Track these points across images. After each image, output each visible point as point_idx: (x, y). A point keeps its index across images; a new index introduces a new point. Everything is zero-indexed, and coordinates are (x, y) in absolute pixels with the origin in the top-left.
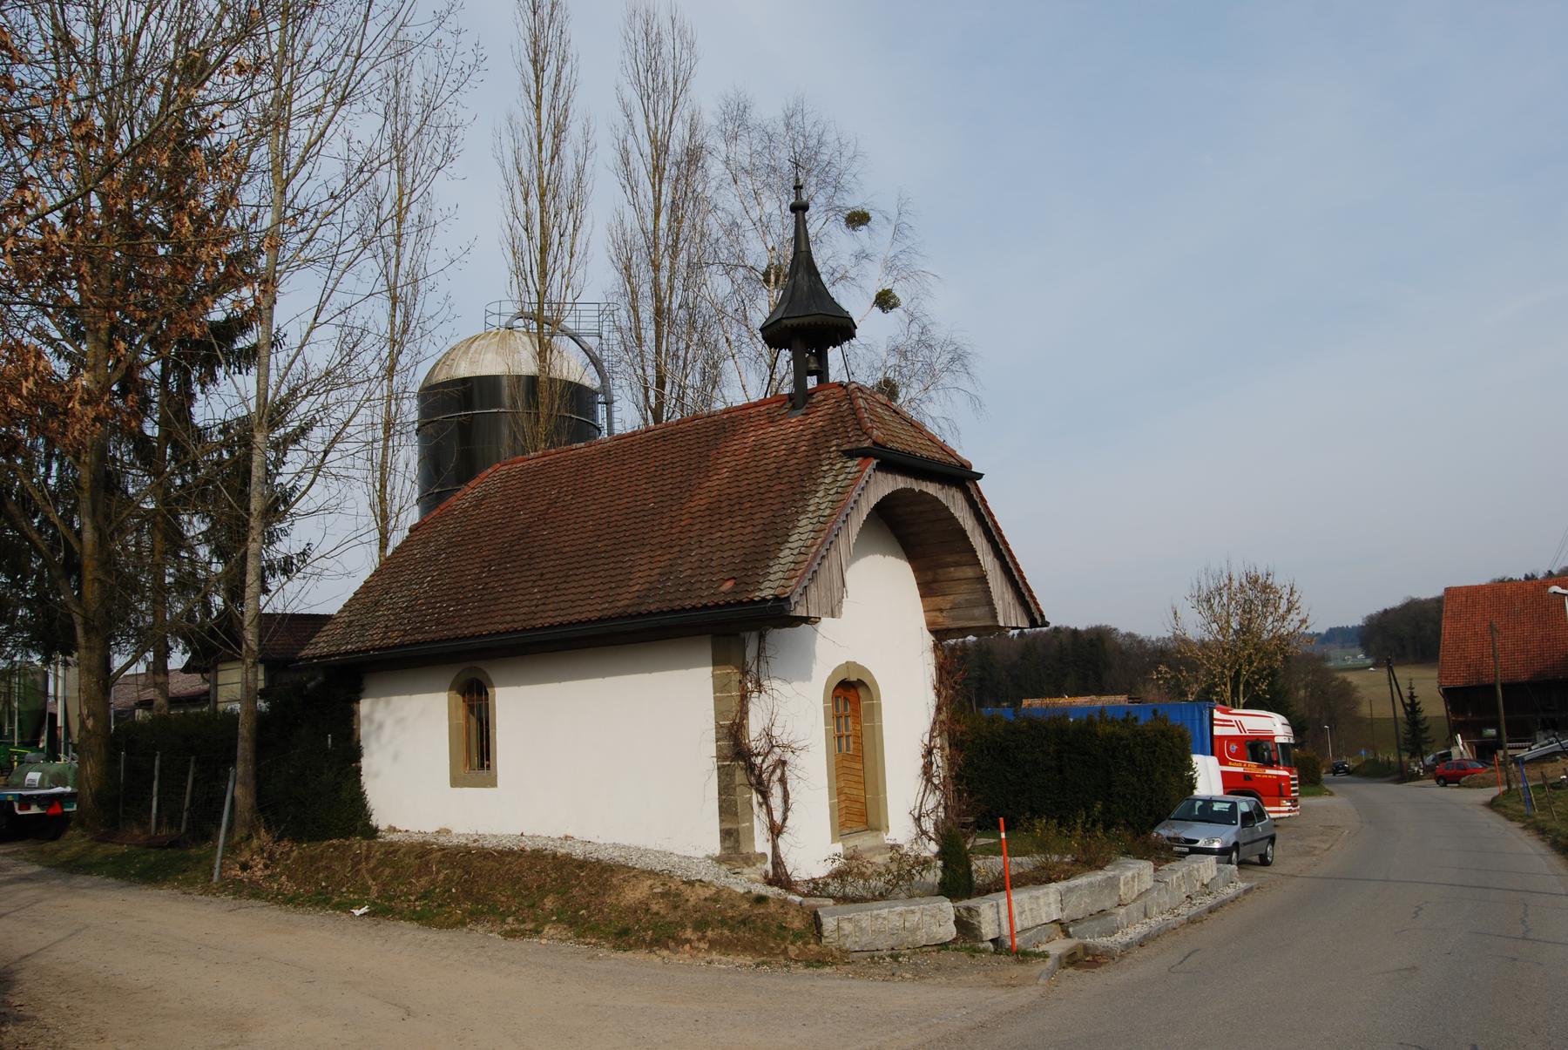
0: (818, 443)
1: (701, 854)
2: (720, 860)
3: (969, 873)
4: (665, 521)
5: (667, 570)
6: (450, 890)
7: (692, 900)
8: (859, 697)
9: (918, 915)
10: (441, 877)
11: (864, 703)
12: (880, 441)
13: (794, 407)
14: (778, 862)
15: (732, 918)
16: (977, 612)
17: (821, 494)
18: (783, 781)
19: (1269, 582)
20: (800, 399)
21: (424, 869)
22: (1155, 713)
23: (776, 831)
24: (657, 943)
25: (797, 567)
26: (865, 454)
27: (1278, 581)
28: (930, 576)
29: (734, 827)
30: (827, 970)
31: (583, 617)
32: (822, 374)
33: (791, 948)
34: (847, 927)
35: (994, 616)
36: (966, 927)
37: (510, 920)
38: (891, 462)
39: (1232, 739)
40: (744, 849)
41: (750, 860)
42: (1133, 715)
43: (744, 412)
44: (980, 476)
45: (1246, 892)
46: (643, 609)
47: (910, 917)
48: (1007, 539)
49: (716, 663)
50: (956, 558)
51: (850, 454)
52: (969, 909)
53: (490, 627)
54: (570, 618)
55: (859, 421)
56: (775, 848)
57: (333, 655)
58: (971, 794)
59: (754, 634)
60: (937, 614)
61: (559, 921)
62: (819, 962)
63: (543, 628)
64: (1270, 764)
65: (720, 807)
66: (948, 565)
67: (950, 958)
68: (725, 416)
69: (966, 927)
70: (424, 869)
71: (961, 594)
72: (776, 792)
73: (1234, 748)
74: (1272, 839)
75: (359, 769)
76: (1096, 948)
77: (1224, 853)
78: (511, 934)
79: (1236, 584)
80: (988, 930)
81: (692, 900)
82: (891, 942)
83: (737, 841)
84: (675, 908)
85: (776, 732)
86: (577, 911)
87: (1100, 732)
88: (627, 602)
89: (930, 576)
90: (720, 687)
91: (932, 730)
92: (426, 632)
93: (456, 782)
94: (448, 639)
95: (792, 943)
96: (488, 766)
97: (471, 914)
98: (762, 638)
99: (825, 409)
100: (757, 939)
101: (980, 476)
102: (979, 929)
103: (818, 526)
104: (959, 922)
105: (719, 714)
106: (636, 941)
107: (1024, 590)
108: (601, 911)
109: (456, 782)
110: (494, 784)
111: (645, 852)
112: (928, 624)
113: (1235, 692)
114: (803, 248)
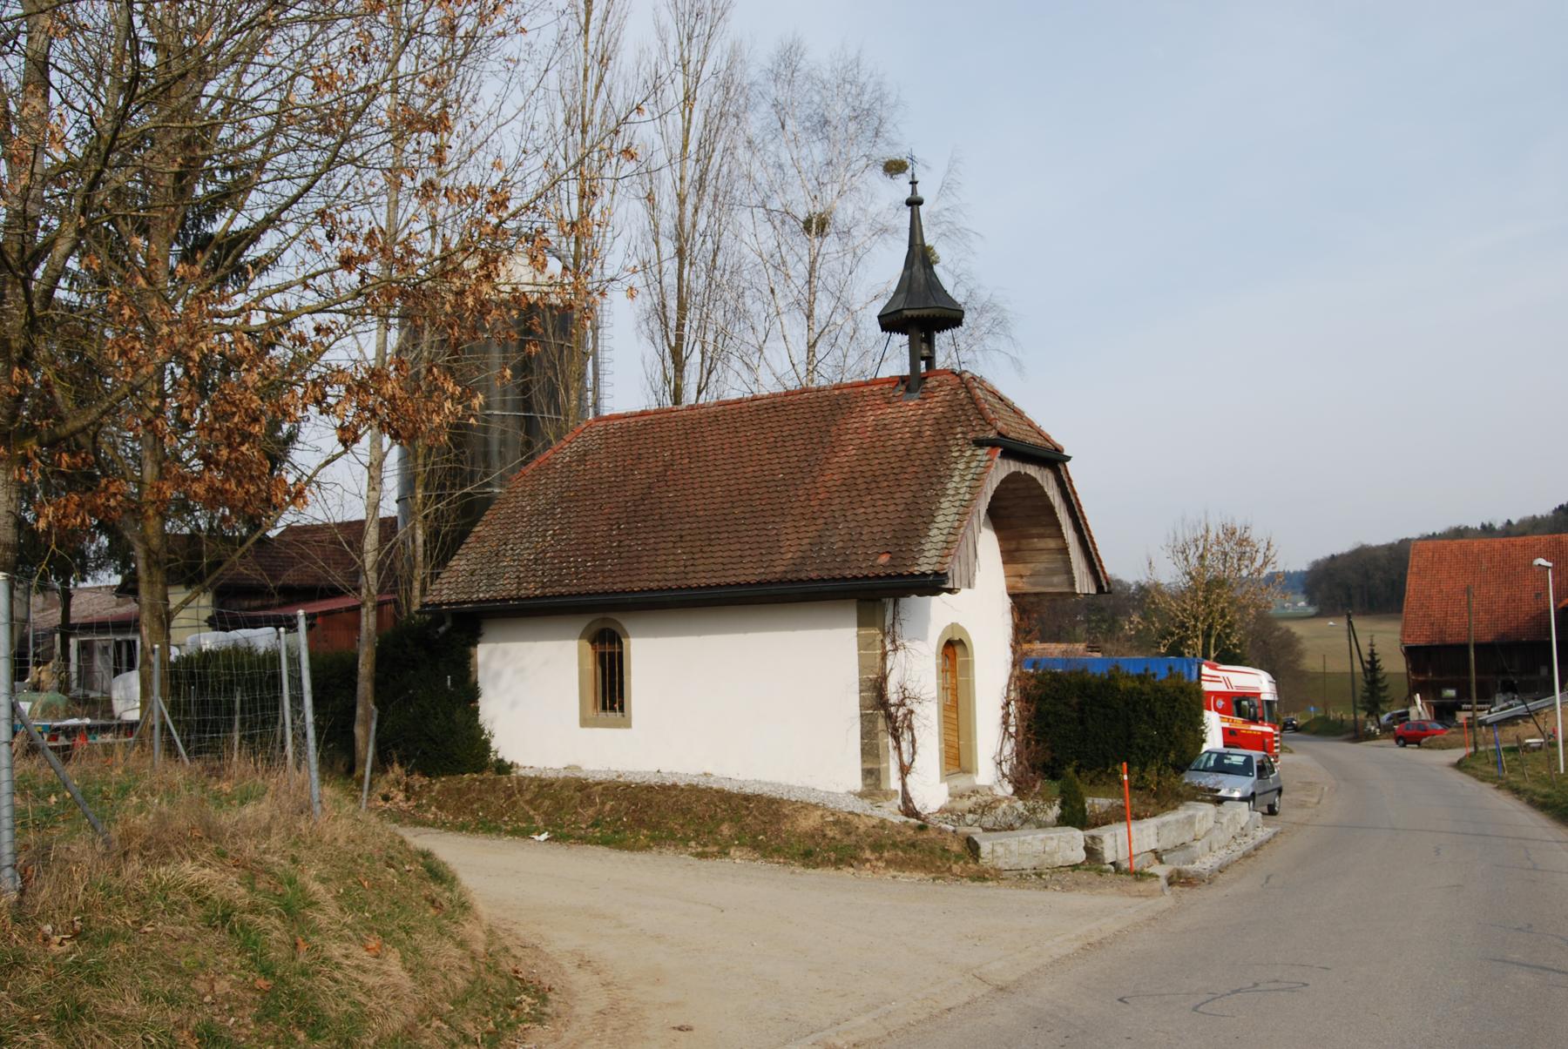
0: (943, 429)
1: (842, 790)
2: (861, 795)
3: (1084, 810)
4: (800, 493)
5: (817, 540)
6: (621, 819)
7: (862, 828)
8: (955, 654)
9: (1056, 841)
10: (608, 807)
11: (960, 659)
12: (1004, 432)
13: (908, 390)
14: (907, 799)
15: (902, 842)
16: (1056, 579)
17: (956, 479)
18: (910, 728)
19: (1246, 535)
20: (910, 384)
21: (588, 800)
22: (1170, 669)
23: (905, 770)
24: (838, 863)
25: (950, 546)
26: (992, 444)
27: (1256, 535)
28: (1013, 545)
29: (875, 766)
30: (990, 883)
31: (741, 579)
32: (930, 360)
33: (954, 866)
34: (1000, 850)
35: (1072, 584)
36: (1092, 852)
37: (693, 844)
38: (1013, 450)
39: (1218, 694)
40: (883, 786)
41: (888, 795)
42: (1151, 672)
43: (855, 390)
44: (1068, 458)
45: (1275, 835)
46: (803, 576)
47: (1049, 843)
48: (1086, 515)
49: (861, 624)
50: (1041, 530)
51: (980, 443)
52: (1093, 838)
53: (641, 584)
54: (728, 580)
55: (980, 412)
56: (904, 785)
57: (465, 602)
58: (1038, 742)
59: (892, 600)
60: (1018, 579)
61: (741, 845)
62: (981, 877)
63: (699, 587)
64: (1254, 720)
65: (862, 750)
66: (1032, 536)
67: (1083, 876)
68: (837, 392)
69: (1092, 852)
70: (588, 800)
71: (1042, 563)
72: (907, 736)
73: (1220, 703)
74: (1280, 791)
75: (477, 709)
76: (1188, 872)
77: (1249, 798)
78: (702, 855)
79: (1212, 536)
80: (1109, 856)
81: (862, 828)
82: (1034, 863)
83: (878, 779)
84: (849, 834)
85: (909, 685)
86: (755, 837)
87: (1122, 687)
88: (784, 568)
89: (1013, 545)
90: (864, 645)
91: (1009, 685)
92: (567, 585)
93: (585, 722)
94: (597, 593)
95: (956, 863)
96: (622, 709)
97: (653, 839)
98: (896, 604)
99: (941, 395)
100: (927, 859)
101: (1068, 458)
102: (1102, 853)
103: (962, 510)
104: (1088, 849)
105: (863, 668)
106: (822, 861)
107: (1096, 560)
108: (778, 836)
109: (585, 722)
110: (628, 725)
111: (791, 789)
112: (1008, 588)
113: (1206, 647)
114: (918, 242)
